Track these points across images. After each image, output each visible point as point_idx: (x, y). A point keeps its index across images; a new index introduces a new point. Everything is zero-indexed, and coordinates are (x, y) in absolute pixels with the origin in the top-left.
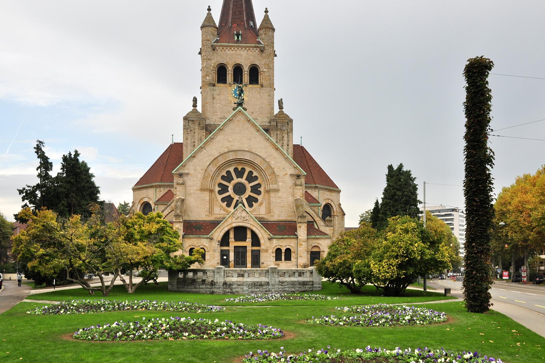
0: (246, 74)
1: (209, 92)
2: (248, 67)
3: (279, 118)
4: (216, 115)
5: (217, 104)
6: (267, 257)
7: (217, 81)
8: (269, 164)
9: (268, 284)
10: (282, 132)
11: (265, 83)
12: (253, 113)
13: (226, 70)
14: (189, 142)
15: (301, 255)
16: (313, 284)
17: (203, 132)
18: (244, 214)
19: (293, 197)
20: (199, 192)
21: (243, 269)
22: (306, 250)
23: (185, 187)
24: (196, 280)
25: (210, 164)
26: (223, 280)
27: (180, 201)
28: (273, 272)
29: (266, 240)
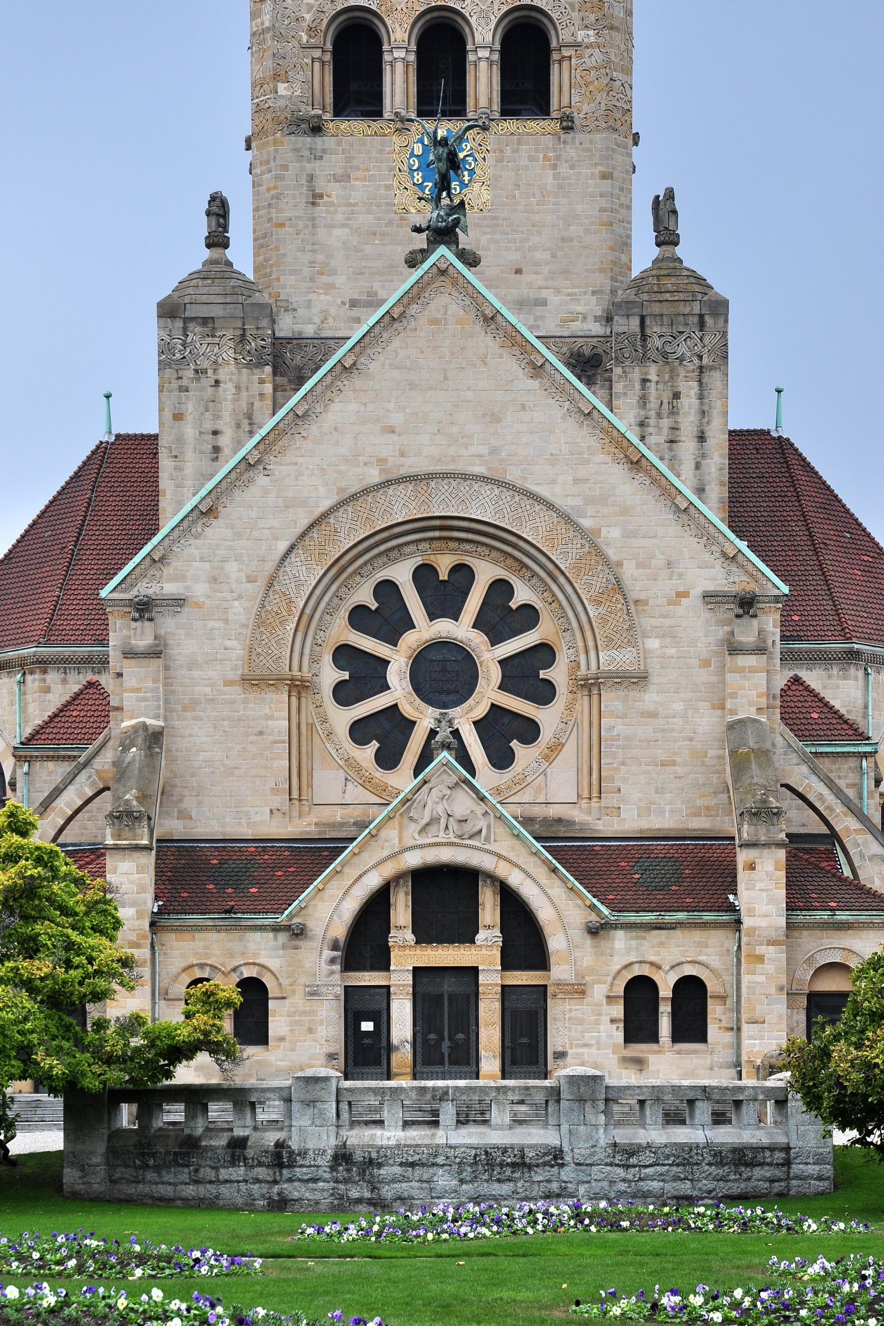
0: (483, 65)
1: (293, 167)
3: (655, 297)
4: (330, 287)
5: (332, 226)
6: (581, 1022)
7: (330, 107)
8: (594, 545)
9: (555, 1158)
10: (672, 371)
11: (586, 108)
12: (518, 271)
13: (380, 44)
14: (189, 431)
15: (757, 1015)
16: (787, 1163)
17: (262, 382)
18: (463, 803)
19: (719, 712)
20: (236, 692)
21: (430, 1083)
22: (781, 989)
23: (167, 668)
24: (199, 1139)
25: (292, 548)
26: (333, 1142)
27: (139, 741)
28: (581, 1101)
29: (578, 935)
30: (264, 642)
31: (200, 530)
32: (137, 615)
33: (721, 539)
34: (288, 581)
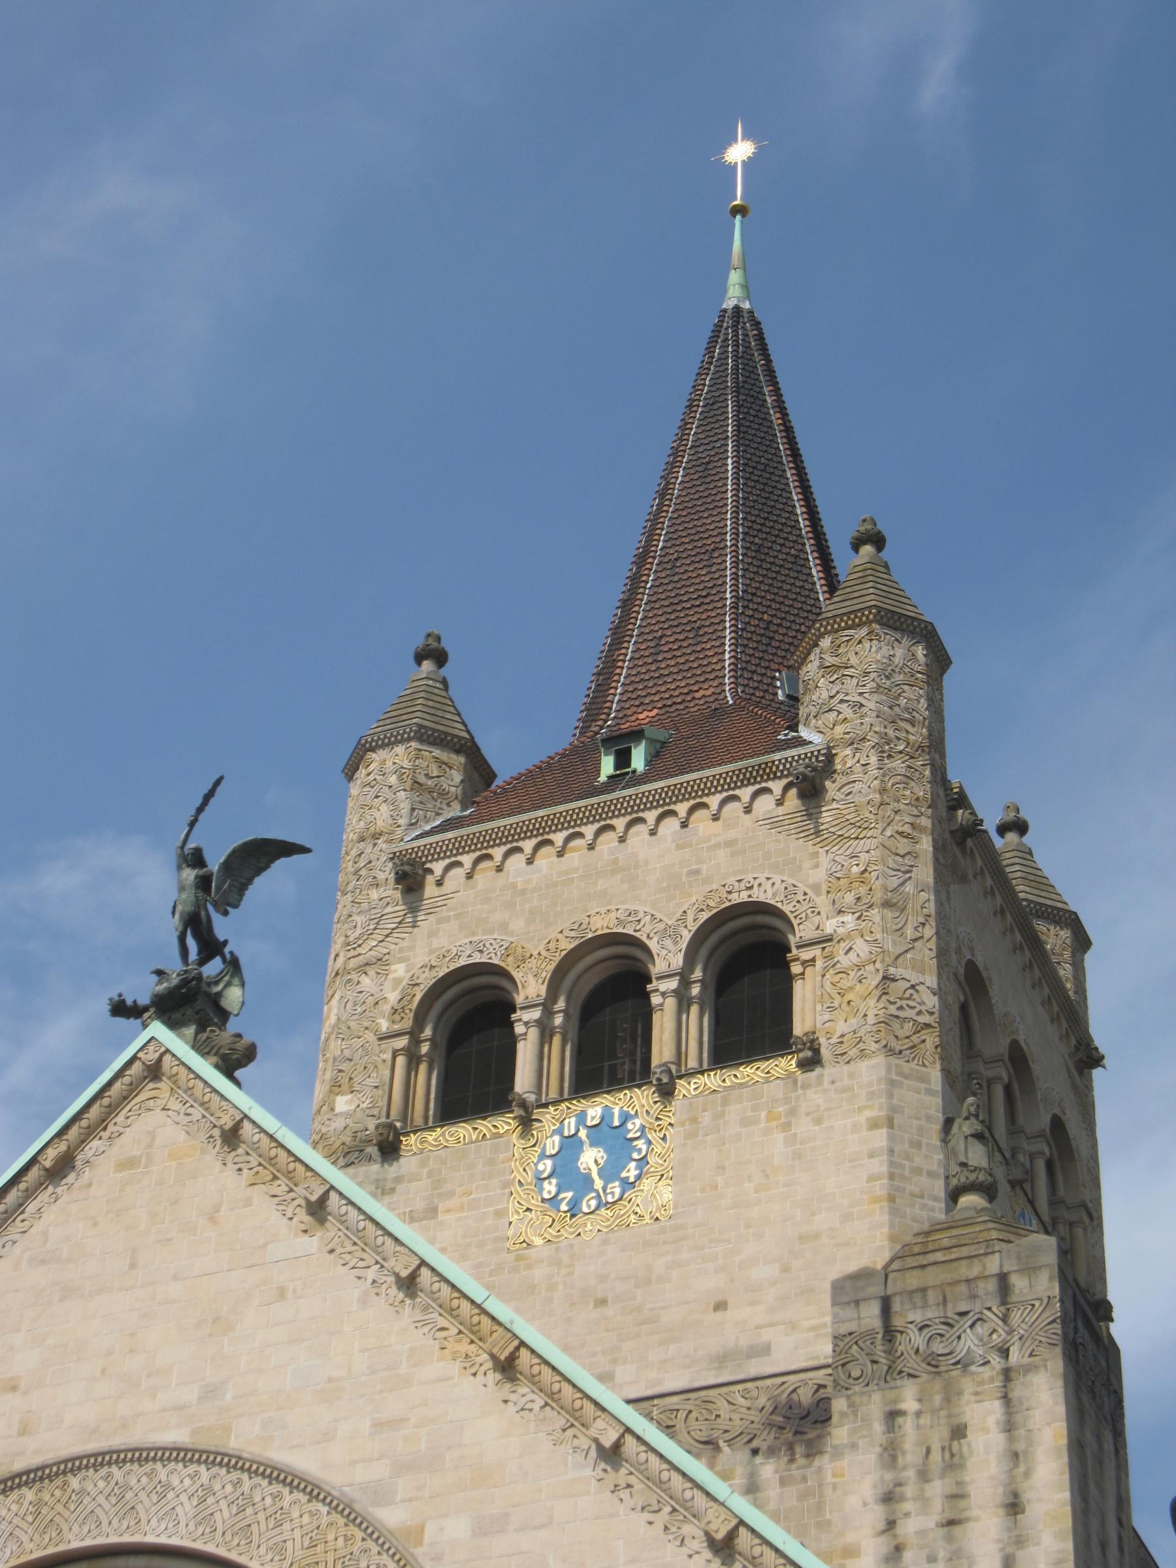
2: (687, 936)
11: (841, 1027)
12: (720, 1306)
33: (700, 1501)
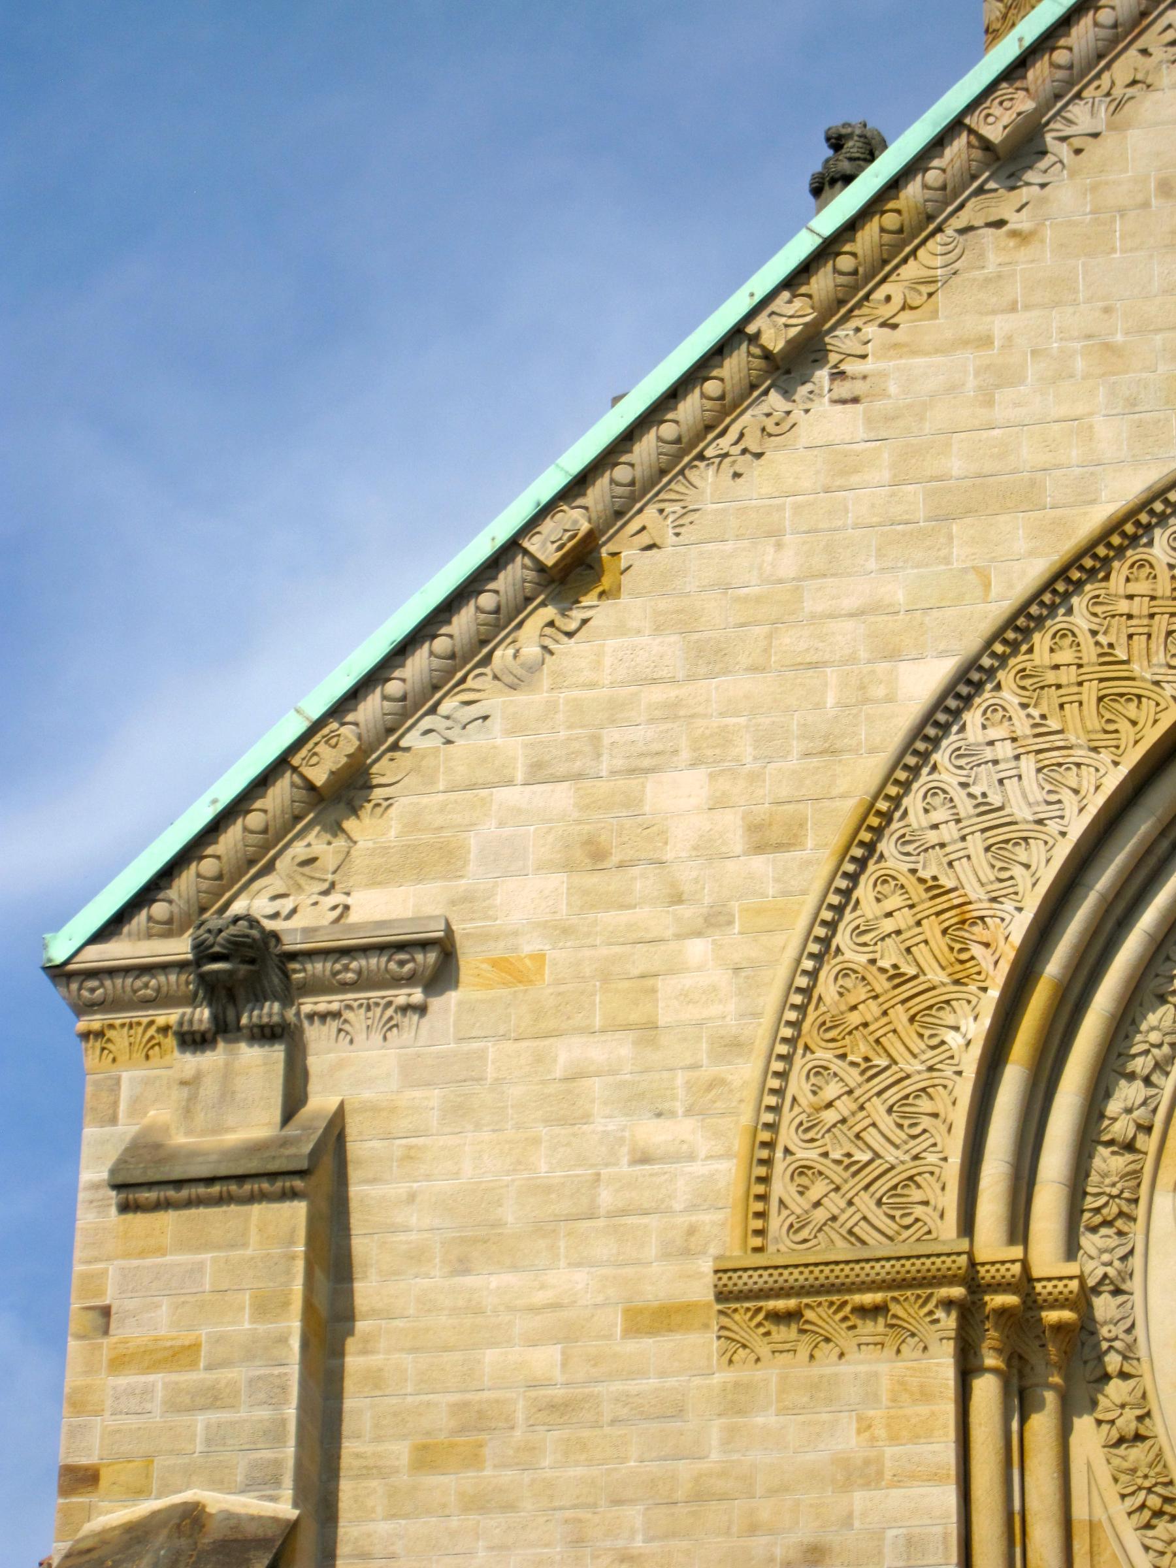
30: (830, 1116)
31: (531, 651)
32: (203, 1015)
34: (949, 832)
